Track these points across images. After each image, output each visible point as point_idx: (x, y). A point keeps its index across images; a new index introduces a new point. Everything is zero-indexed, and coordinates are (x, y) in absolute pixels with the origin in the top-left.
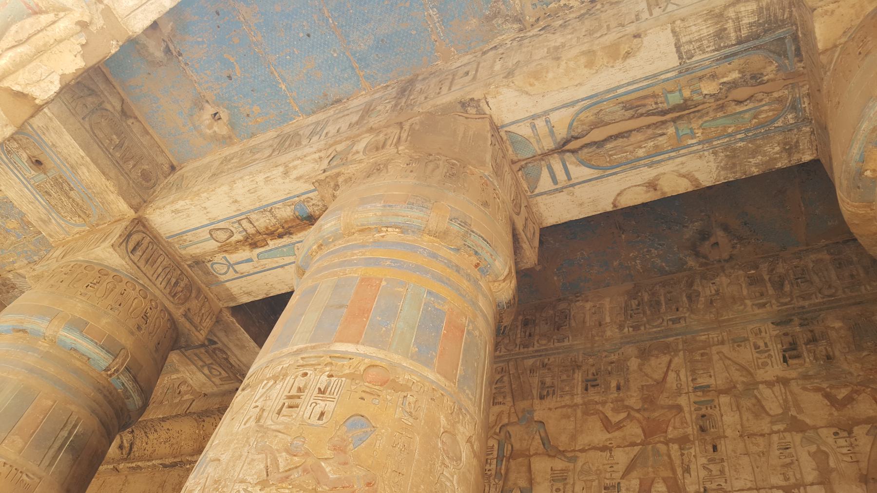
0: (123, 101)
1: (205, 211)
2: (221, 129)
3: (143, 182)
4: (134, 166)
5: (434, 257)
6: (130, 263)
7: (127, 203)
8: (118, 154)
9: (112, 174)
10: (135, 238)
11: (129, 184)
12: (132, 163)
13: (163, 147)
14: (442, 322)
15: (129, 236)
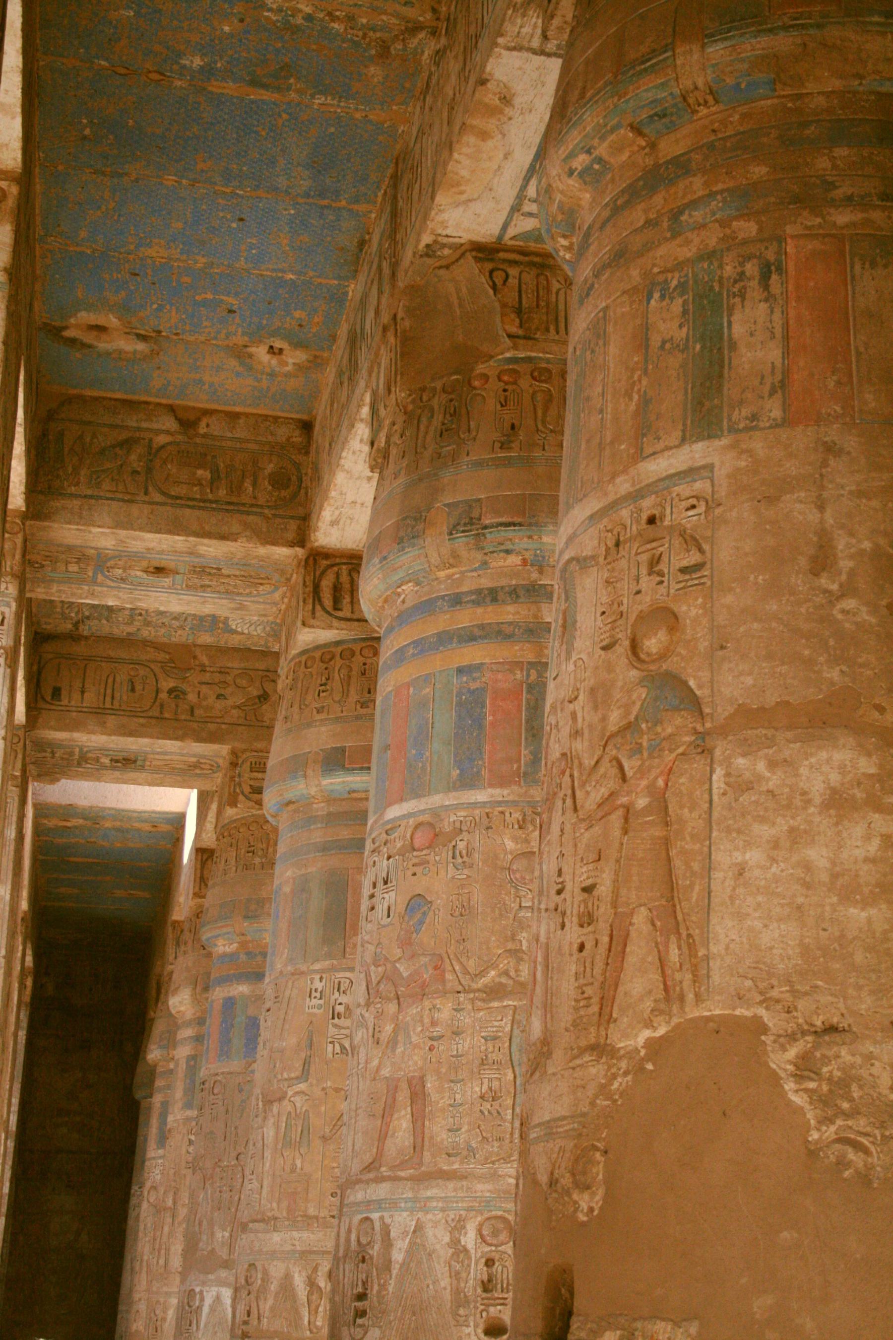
0: (172, 409)
1: (358, 506)
2: (294, 358)
3: (283, 493)
4: (254, 484)
5: (457, 603)
6: (343, 624)
7: (283, 545)
8: (222, 492)
9: (236, 528)
10: (326, 584)
11: (266, 518)
12: (248, 485)
13: (271, 413)
14: (483, 706)
15: (317, 589)
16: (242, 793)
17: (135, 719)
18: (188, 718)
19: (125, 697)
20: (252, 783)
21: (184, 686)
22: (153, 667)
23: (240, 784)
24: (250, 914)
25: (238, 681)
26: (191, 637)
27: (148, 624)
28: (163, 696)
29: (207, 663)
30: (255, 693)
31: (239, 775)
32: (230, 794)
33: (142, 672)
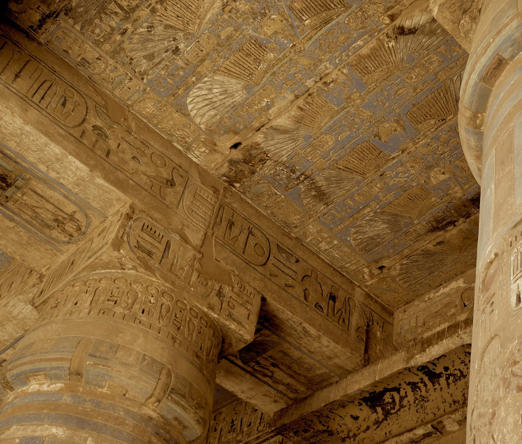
16: (129, 243)
17: (57, 127)
18: (103, 156)
19: (54, 105)
20: (140, 240)
21: (108, 132)
22: (88, 101)
23: (128, 236)
24: (98, 354)
25: (154, 158)
26: (135, 97)
27: (115, 53)
28: (88, 126)
29: (134, 129)
30: (165, 175)
31: (131, 227)
32: (117, 236)
33: (76, 98)
